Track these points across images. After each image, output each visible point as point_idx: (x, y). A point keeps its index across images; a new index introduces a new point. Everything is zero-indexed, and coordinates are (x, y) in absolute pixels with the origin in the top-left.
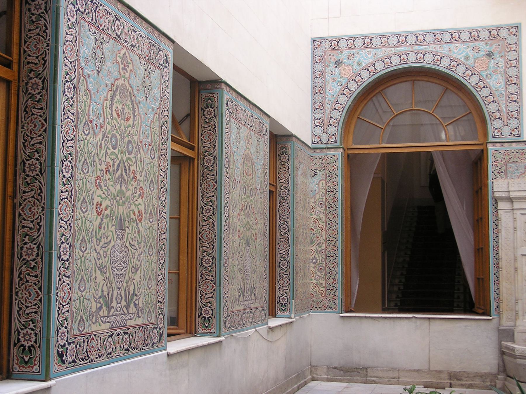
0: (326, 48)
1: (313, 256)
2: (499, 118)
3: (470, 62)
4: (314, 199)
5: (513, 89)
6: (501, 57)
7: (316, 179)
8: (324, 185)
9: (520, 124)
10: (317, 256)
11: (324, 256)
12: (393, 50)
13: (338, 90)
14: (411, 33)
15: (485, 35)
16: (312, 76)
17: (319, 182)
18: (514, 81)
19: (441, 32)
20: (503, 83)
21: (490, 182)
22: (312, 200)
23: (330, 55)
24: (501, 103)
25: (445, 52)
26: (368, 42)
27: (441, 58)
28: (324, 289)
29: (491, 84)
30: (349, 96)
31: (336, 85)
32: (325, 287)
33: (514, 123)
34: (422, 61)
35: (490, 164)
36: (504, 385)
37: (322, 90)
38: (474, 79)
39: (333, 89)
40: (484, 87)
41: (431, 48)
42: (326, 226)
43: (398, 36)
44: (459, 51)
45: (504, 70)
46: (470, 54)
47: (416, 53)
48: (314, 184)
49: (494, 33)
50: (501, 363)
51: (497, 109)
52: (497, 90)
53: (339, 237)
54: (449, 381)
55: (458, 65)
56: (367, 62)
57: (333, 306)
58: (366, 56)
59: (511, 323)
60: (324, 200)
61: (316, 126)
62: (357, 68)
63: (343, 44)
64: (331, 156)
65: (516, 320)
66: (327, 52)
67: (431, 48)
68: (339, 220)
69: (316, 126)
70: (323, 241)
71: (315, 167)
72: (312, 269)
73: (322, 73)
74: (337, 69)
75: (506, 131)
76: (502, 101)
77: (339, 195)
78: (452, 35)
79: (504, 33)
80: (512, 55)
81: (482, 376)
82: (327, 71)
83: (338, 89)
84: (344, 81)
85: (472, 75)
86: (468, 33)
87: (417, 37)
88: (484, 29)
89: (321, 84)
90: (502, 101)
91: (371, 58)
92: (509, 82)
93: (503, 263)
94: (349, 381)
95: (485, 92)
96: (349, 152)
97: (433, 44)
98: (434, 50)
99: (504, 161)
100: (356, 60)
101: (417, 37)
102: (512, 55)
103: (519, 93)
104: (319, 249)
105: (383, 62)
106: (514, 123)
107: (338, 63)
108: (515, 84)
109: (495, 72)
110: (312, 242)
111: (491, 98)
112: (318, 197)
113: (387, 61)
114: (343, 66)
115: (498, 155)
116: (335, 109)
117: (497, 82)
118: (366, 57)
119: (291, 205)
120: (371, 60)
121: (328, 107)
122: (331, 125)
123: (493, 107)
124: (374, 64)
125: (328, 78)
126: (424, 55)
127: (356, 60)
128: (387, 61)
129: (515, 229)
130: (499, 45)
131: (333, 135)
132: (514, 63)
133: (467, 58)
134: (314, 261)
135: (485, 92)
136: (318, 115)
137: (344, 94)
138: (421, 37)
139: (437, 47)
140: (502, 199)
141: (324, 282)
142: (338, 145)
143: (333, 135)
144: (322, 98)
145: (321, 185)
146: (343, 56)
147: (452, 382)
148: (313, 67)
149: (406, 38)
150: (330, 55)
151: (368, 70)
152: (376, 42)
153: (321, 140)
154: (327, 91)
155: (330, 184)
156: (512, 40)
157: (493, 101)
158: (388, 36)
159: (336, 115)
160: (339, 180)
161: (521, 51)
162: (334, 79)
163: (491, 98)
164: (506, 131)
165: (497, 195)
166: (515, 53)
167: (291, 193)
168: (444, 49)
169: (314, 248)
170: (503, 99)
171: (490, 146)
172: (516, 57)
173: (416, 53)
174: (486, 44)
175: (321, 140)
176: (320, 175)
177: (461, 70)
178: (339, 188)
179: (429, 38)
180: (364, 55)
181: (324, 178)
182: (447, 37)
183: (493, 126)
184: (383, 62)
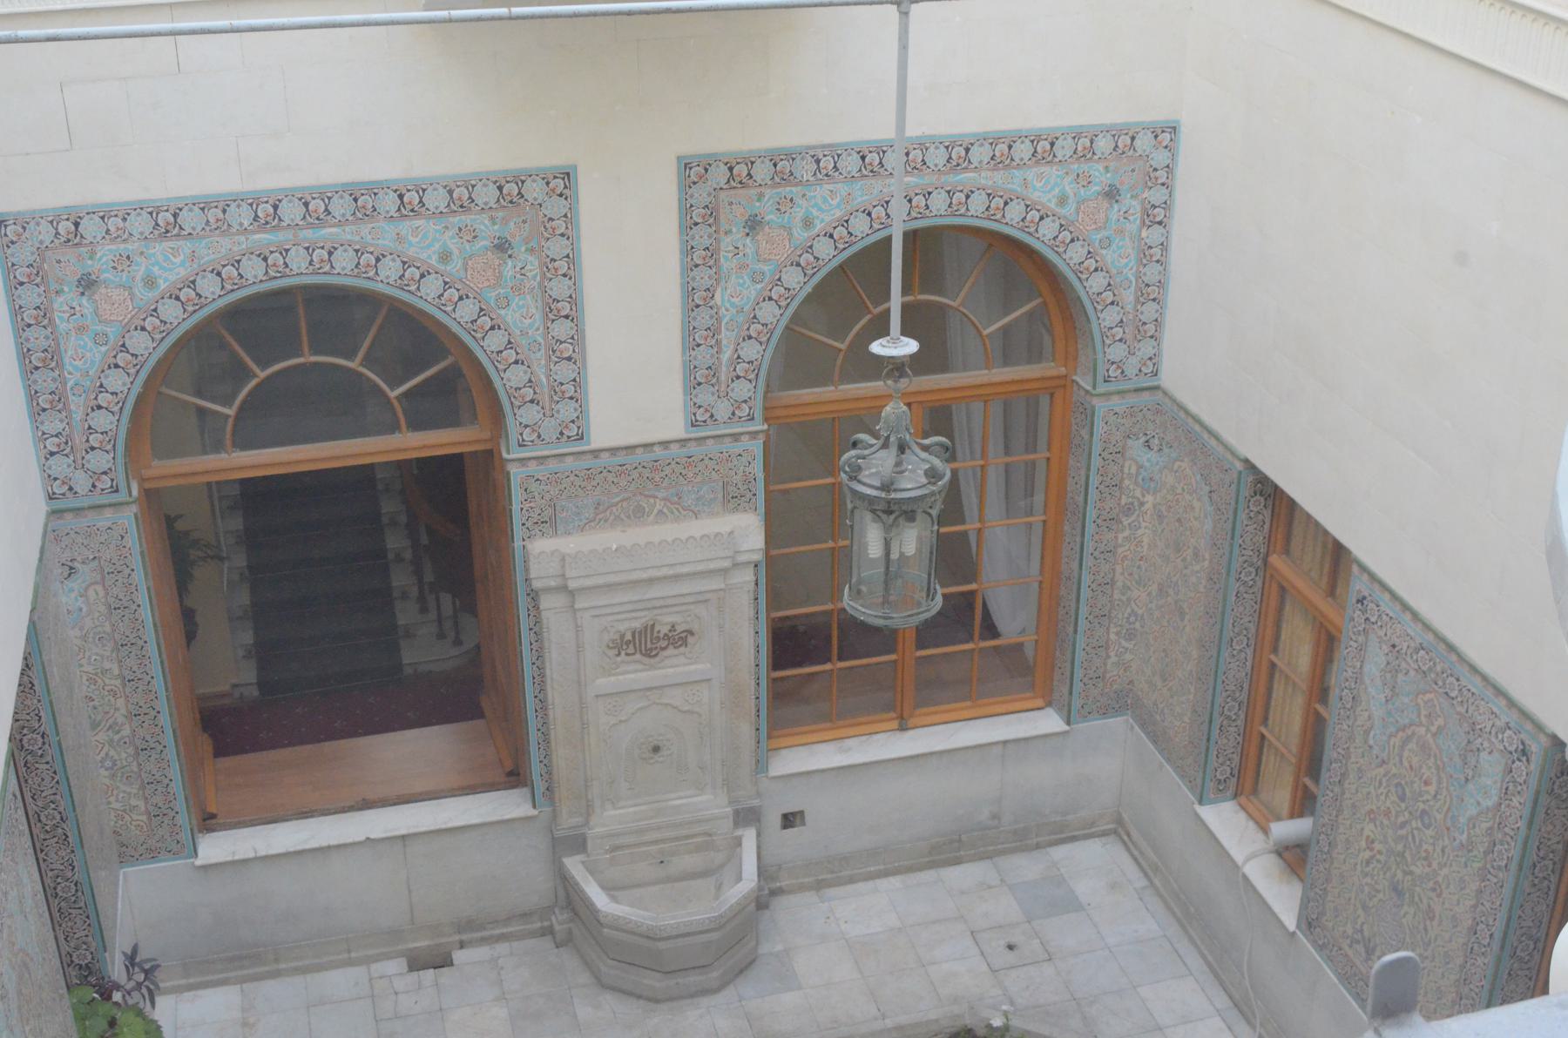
0: (41, 242)
1: (103, 754)
2: (532, 401)
3: (454, 267)
4: (81, 629)
5: (562, 329)
6: (532, 250)
7: (76, 584)
8: (102, 593)
9: (582, 412)
10: (112, 753)
11: (131, 750)
12: (243, 243)
13: (98, 357)
14: (289, 193)
15: (487, 195)
16: (14, 323)
17: (86, 589)
18: (565, 311)
19: (373, 189)
20: (538, 316)
21: (518, 544)
22: (78, 633)
23: (59, 262)
24: (534, 367)
25: (386, 242)
26: (167, 221)
27: (378, 260)
28: (144, 818)
29: (509, 319)
30: (132, 371)
31: (90, 344)
32: (148, 813)
33: (567, 411)
34: (327, 268)
35: (515, 507)
36: (570, 932)
37: (53, 358)
38: (467, 311)
39: (82, 357)
40: (492, 328)
41: (348, 233)
42: (124, 686)
43: (254, 201)
44: (425, 240)
45: (541, 284)
46: (453, 245)
47: (307, 249)
48: (73, 595)
49: (510, 190)
50: (561, 893)
51: (526, 378)
52: (524, 333)
53: (163, 704)
54: (457, 938)
55: (422, 276)
56: (172, 278)
57: (174, 847)
58: (167, 259)
59: (578, 820)
60: (108, 629)
61: (52, 454)
62: (145, 296)
63: (90, 228)
64: (109, 524)
65: (589, 815)
66: (48, 253)
67: (348, 233)
68: (156, 669)
69: (52, 454)
70: (121, 720)
71: (67, 555)
72: (107, 781)
73: (44, 314)
74: (84, 301)
75: (549, 428)
76: (539, 359)
77: (146, 614)
78: (401, 197)
79: (534, 190)
80: (557, 247)
81: (525, 916)
82: (56, 306)
83: (97, 355)
84: (113, 332)
85: (461, 298)
86: (443, 192)
87: (306, 204)
88: (485, 178)
89: (45, 344)
90: (539, 359)
91: (182, 264)
92: (551, 312)
93: (557, 712)
94: (242, 981)
95: (495, 341)
96: (147, 485)
97: (353, 223)
98: (357, 238)
99: (547, 497)
100: (140, 271)
101: (306, 204)
102: (557, 247)
103: (578, 339)
104: (117, 737)
105: (219, 274)
106: (567, 411)
107: (87, 284)
108: (567, 317)
109: (517, 289)
110: (95, 725)
111: (511, 355)
112: (88, 623)
113: (229, 271)
114: (103, 291)
115: (534, 487)
116: (99, 407)
117: (522, 315)
118: (169, 264)
119: (58, 766)
120: (183, 272)
121: (77, 405)
122: (93, 448)
123: (516, 376)
124: (193, 282)
125: (62, 326)
126: (330, 254)
127: (140, 271)
128: (229, 271)
129: (579, 648)
130: (524, 222)
131: (105, 473)
132: (563, 266)
133: (445, 257)
134: (108, 763)
135: (495, 341)
136: (53, 424)
137: (117, 366)
138: (317, 205)
139: (365, 229)
140: (548, 590)
141: (141, 804)
142: (122, 496)
143: (105, 473)
144: (54, 380)
145: (91, 592)
146: (102, 260)
147: (465, 937)
148: (11, 299)
149: (275, 207)
150: (59, 262)
151: (178, 298)
152: (190, 220)
153: (71, 489)
154: (66, 360)
155: (115, 591)
156: (555, 207)
157: (516, 362)
158: (224, 204)
159: (102, 421)
160: (139, 577)
161: (579, 237)
162: (81, 329)
163: (511, 355)
164: (549, 428)
165: (536, 584)
166: (564, 241)
167: (53, 739)
168: (383, 235)
169: (102, 737)
170: (538, 355)
171: (515, 471)
172: (569, 251)
173: (307, 249)
174: (492, 218)
175: (71, 489)
176: (86, 572)
177: (431, 287)
178: (143, 598)
179: (341, 207)
180: (160, 258)
181: (99, 577)
182: (389, 203)
183: (520, 418)
184: (219, 274)
